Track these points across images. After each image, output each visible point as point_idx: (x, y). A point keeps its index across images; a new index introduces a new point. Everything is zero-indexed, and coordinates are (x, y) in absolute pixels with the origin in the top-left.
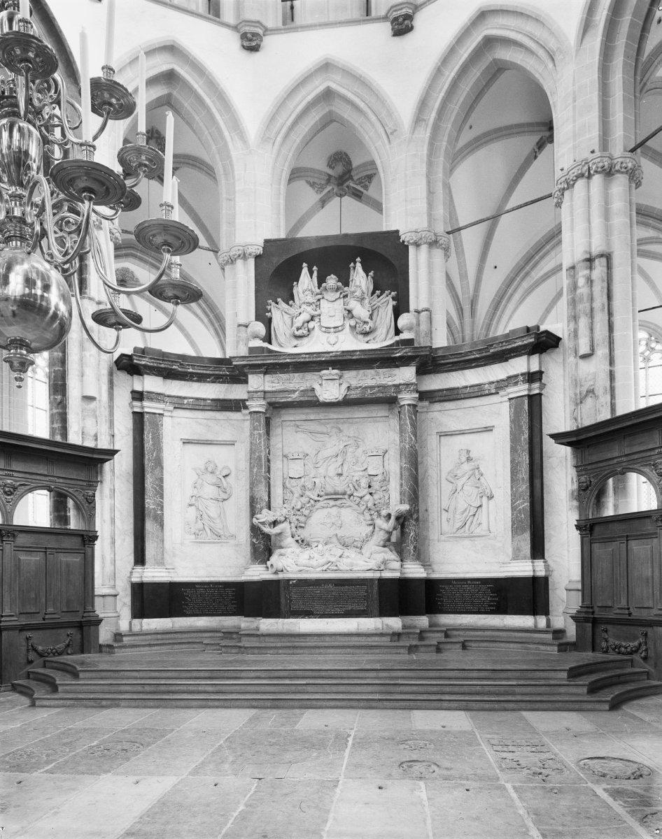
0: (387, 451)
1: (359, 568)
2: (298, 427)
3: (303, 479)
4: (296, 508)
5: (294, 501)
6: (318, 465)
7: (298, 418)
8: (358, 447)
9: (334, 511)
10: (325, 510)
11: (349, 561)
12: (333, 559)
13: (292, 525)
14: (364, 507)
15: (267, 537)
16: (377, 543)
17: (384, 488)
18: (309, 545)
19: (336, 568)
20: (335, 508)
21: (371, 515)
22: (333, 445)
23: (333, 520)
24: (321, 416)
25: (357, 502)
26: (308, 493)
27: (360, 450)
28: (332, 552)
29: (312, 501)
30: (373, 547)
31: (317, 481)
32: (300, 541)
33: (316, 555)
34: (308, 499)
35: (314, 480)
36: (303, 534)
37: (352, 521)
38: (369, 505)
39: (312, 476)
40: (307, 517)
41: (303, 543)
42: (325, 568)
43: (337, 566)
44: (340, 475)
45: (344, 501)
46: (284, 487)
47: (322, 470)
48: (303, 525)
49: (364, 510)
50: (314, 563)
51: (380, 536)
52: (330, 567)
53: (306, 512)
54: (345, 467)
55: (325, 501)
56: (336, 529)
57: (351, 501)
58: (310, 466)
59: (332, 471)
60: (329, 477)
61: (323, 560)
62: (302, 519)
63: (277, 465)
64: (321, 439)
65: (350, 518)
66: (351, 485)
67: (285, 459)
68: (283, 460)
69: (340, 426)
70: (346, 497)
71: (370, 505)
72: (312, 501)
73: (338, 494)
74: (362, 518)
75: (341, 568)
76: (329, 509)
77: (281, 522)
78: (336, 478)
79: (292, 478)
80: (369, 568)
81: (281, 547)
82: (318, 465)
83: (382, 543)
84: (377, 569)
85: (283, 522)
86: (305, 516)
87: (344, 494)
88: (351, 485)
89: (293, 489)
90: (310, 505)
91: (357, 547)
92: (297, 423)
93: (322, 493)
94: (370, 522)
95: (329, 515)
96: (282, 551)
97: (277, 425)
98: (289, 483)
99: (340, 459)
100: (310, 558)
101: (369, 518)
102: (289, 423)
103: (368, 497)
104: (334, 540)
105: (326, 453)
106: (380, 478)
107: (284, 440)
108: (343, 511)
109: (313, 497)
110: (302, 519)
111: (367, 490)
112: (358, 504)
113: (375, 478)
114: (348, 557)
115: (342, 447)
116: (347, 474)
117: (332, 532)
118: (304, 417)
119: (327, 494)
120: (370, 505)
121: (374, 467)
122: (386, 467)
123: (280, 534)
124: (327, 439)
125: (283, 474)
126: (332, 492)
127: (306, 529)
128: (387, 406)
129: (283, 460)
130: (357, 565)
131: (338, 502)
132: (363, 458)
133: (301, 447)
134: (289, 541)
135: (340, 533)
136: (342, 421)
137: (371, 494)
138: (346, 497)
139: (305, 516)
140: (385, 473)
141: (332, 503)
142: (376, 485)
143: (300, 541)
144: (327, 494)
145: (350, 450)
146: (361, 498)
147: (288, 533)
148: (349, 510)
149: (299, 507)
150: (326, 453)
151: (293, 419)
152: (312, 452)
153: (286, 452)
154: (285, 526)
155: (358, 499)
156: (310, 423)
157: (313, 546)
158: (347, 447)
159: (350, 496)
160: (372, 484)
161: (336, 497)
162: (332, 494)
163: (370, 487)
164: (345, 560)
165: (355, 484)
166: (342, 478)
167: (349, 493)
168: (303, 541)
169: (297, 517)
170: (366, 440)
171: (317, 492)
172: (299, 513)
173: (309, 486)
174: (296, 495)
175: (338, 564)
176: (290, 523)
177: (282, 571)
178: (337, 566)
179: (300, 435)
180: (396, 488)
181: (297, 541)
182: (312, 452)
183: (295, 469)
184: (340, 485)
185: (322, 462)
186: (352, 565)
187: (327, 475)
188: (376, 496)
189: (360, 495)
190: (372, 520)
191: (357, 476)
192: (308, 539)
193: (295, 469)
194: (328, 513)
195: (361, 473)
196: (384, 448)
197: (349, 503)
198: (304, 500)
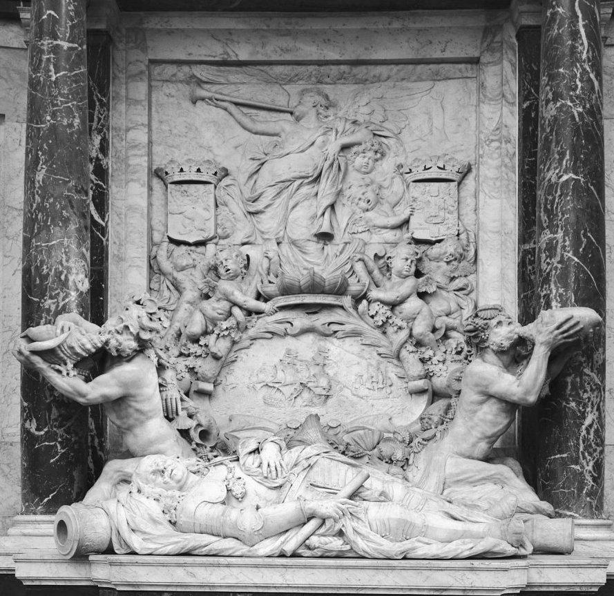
0: (469, 170)
1: (435, 549)
2: (200, 83)
3: (211, 247)
4: (186, 332)
5: (181, 314)
6: (259, 206)
7: (200, 53)
8: (381, 154)
9: (306, 346)
10: (277, 342)
11: (391, 512)
12: (327, 506)
13: (169, 375)
14: (403, 335)
15: (70, 408)
16: (465, 447)
17: (459, 283)
18: (225, 450)
19: (336, 544)
20: (309, 338)
21: (423, 361)
22: (304, 144)
23: (304, 376)
24: (271, 50)
25: (380, 319)
26: (225, 286)
27: (387, 165)
28: (316, 476)
29: (236, 311)
30: (449, 461)
31: (254, 253)
32: (195, 435)
33: (255, 489)
34: (225, 305)
35: (246, 250)
36: (211, 413)
37: (360, 377)
38: (415, 332)
39: (239, 237)
40: (223, 362)
41: (206, 442)
42: (291, 542)
43: (341, 533)
44: (325, 237)
45: (337, 316)
46: (154, 268)
47: (269, 222)
48: (208, 387)
49: (402, 346)
50: (246, 518)
51: (478, 422)
52: (314, 541)
53: (221, 347)
54: (343, 214)
55: (280, 316)
56: (311, 404)
57: (361, 317)
58: (237, 207)
59: (302, 222)
60: (293, 243)
61: (287, 509)
62: (207, 367)
63: (130, 196)
64: (271, 128)
65: (356, 369)
66: (359, 267)
67: (157, 184)
68: (150, 189)
69: (328, 89)
70: (347, 301)
71: (420, 328)
72: (236, 311)
73: (323, 292)
74: (392, 371)
75: (362, 545)
76: (290, 342)
77: (121, 358)
78: (313, 247)
79: (178, 243)
80: (480, 548)
81: (129, 454)
82: (259, 206)
83: (483, 446)
84: (511, 550)
85: (129, 359)
86: (216, 358)
87: (341, 290)
88: (359, 267)
89: (180, 276)
90: (231, 322)
91: (391, 461)
92: (200, 72)
93: (271, 289)
94: (421, 384)
95: (291, 360)
96: (128, 465)
97: (133, 69)
98: (170, 255)
99: (326, 189)
100: (231, 497)
101: (416, 369)
102: (170, 70)
103: (414, 304)
104: (312, 433)
105: (282, 168)
106: (449, 248)
107: (155, 125)
108: (335, 348)
109: (239, 297)
110: (207, 367)
111: (411, 282)
112: (383, 327)
113: (435, 250)
114: (384, 497)
115: (333, 147)
116: (347, 238)
117: (299, 411)
118: (215, 50)
119: (286, 290)
120: (420, 328)
121: (431, 214)
122: (469, 219)
123: (121, 402)
124: (288, 127)
125: (151, 229)
126: (303, 279)
127: (215, 402)
128: (477, 20)
129: (150, 189)
130: (425, 531)
131: (321, 320)
132: (398, 186)
133: (209, 149)
134: (155, 428)
135: (329, 413)
136: (334, 70)
137: (422, 295)
138: (347, 301)
139: (216, 358)
140: (463, 236)
141: (300, 320)
142: (437, 272)
143: (195, 435)
144: (286, 290)
145: (359, 161)
146: (393, 306)
147: (150, 398)
148: (351, 345)
149: (196, 328)
150: (282, 168)
151: (183, 57)
152: (240, 165)
153: (158, 163)
154: (139, 372)
155: (384, 310)
156: (235, 75)
157: (242, 452)
158: (350, 154)
159: (357, 300)
160: (427, 266)
161: (314, 299)
162: (301, 291)
163: (418, 274)
164: (374, 512)
165: (371, 264)
166: (330, 249)
167: (354, 287)
168: (204, 435)
169: (190, 362)
170: (405, 136)
171: (254, 284)
172: (194, 348)
173: (231, 265)
174: (190, 294)
175: (348, 525)
176: (161, 368)
177: (110, 550)
178: (341, 533)
179: (205, 112)
180: (503, 276)
181: (184, 433)
182: (240, 165)
183: (191, 214)
184: (325, 265)
185: (271, 192)
186: (404, 530)
187: (283, 236)
188: (438, 305)
189: (390, 296)
190: (428, 376)
191: (376, 243)
192: (222, 428)
193: (191, 214)
194: (288, 353)
195: (390, 235)
196: (463, 159)
197: (353, 323)
198: (214, 307)
